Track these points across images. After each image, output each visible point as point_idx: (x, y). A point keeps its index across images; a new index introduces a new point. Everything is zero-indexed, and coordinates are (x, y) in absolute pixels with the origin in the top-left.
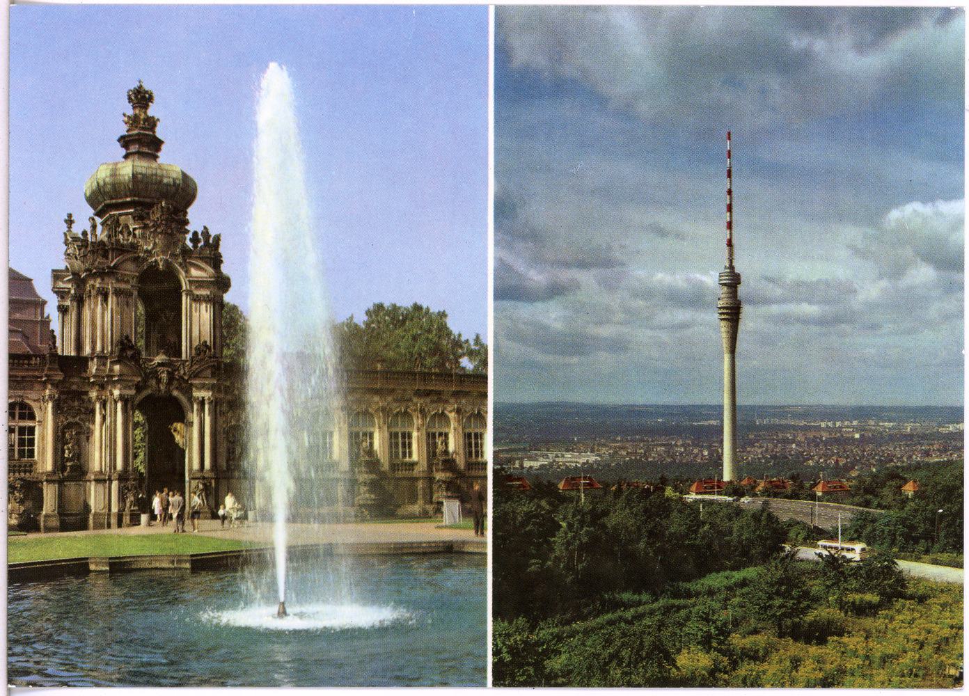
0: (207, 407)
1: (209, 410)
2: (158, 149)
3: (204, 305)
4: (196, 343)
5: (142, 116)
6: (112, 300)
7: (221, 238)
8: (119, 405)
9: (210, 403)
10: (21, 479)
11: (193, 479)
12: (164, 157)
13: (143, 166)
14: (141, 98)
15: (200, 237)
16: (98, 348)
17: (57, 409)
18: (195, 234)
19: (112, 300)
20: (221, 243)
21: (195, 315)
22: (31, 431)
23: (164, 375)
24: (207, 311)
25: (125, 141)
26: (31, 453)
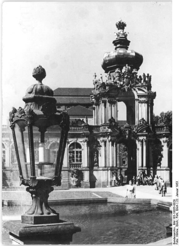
0: (144, 143)
1: (145, 144)
2: (129, 45)
3: (143, 104)
4: (140, 118)
5: (122, 33)
6: (108, 104)
7: (151, 77)
8: (110, 143)
9: (146, 141)
10: (76, 169)
11: (139, 170)
12: (130, 47)
13: (121, 51)
14: (121, 26)
15: (142, 77)
16: (103, 122)
17: (88, 145)
18: (140, 77)
19: (108, 104)
20: (152, 79)
21: (140, 108)
22: (81, 152)
23: (127, 132)
24: (145, 106)
25: (115, 43)
26: (81, 161)
